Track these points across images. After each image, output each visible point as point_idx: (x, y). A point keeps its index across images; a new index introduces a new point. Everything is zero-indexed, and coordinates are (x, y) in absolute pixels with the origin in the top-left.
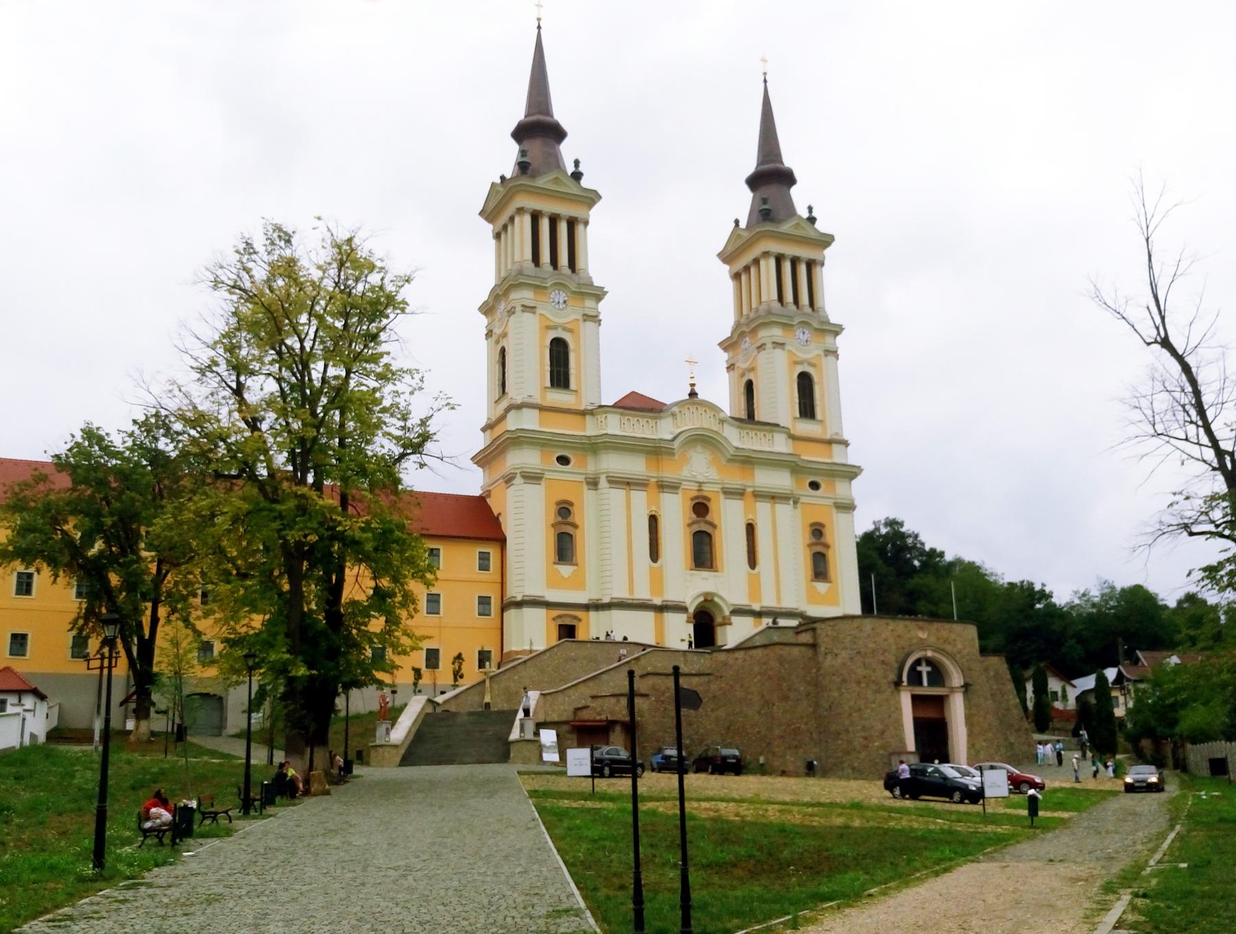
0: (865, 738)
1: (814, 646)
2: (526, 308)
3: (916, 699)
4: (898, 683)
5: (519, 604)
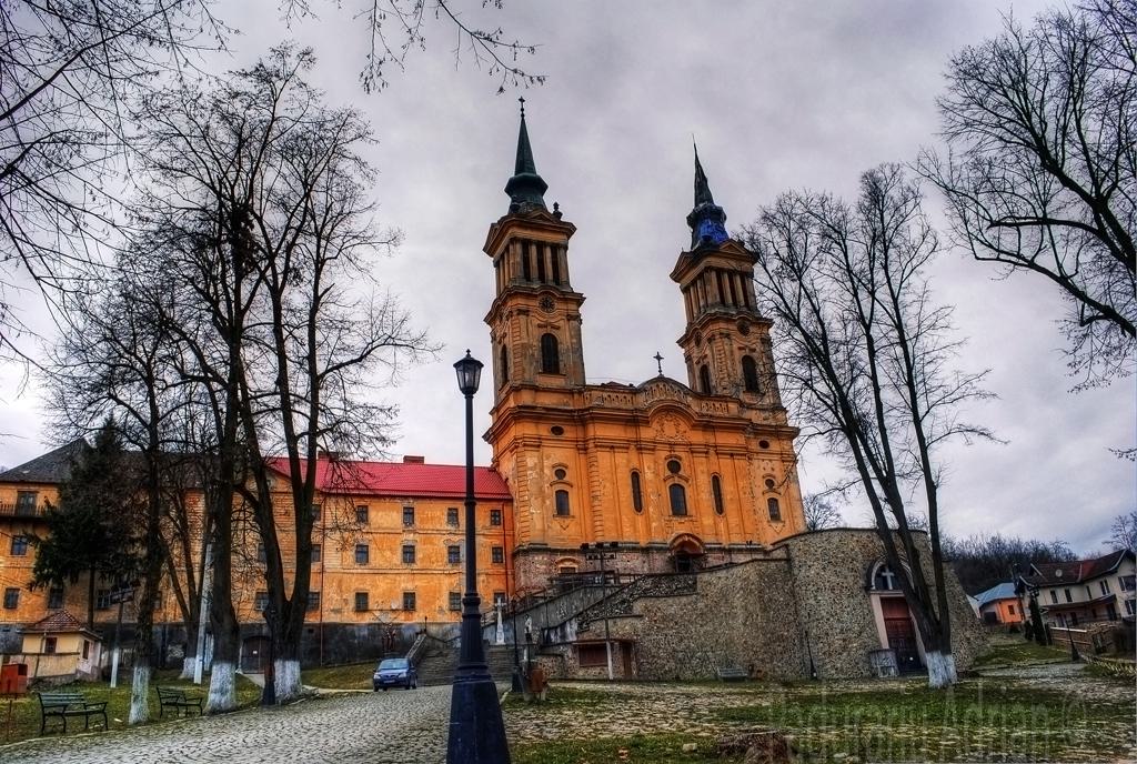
0: (844, 640)
1: (789, 560)
2: (521, 312)
3: (882, 600)
4: (867, 588)
5: (526, 552)
